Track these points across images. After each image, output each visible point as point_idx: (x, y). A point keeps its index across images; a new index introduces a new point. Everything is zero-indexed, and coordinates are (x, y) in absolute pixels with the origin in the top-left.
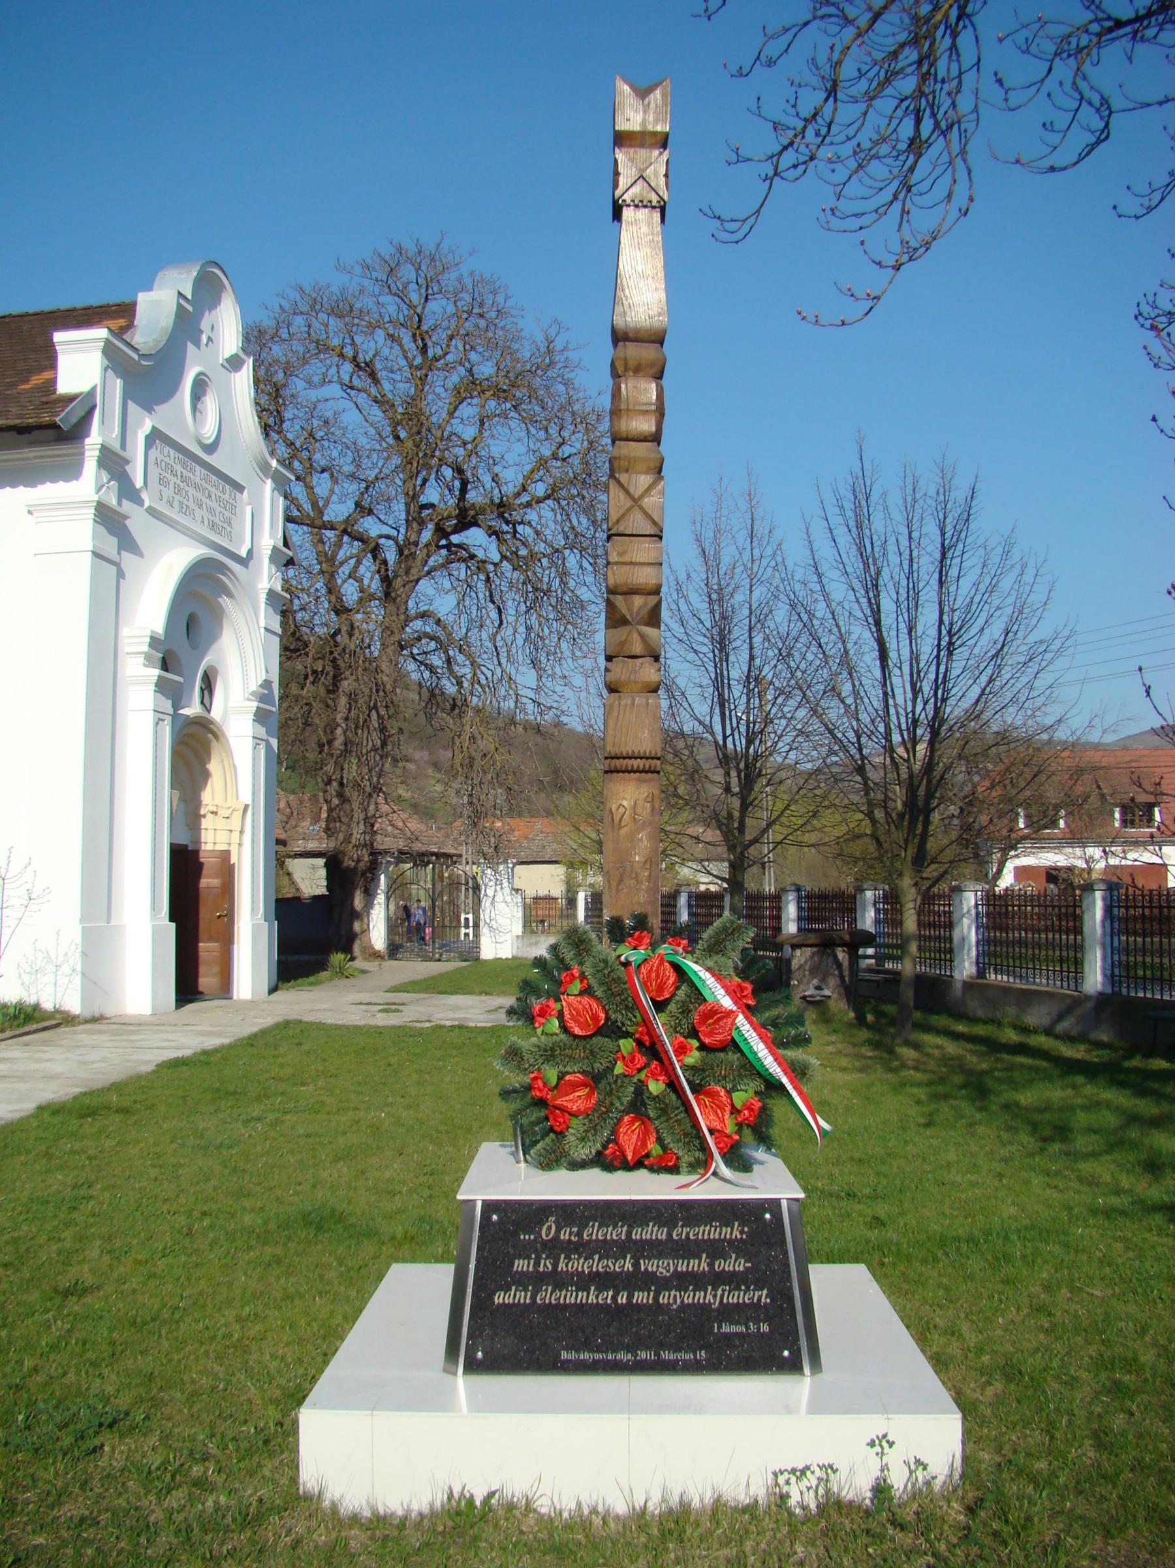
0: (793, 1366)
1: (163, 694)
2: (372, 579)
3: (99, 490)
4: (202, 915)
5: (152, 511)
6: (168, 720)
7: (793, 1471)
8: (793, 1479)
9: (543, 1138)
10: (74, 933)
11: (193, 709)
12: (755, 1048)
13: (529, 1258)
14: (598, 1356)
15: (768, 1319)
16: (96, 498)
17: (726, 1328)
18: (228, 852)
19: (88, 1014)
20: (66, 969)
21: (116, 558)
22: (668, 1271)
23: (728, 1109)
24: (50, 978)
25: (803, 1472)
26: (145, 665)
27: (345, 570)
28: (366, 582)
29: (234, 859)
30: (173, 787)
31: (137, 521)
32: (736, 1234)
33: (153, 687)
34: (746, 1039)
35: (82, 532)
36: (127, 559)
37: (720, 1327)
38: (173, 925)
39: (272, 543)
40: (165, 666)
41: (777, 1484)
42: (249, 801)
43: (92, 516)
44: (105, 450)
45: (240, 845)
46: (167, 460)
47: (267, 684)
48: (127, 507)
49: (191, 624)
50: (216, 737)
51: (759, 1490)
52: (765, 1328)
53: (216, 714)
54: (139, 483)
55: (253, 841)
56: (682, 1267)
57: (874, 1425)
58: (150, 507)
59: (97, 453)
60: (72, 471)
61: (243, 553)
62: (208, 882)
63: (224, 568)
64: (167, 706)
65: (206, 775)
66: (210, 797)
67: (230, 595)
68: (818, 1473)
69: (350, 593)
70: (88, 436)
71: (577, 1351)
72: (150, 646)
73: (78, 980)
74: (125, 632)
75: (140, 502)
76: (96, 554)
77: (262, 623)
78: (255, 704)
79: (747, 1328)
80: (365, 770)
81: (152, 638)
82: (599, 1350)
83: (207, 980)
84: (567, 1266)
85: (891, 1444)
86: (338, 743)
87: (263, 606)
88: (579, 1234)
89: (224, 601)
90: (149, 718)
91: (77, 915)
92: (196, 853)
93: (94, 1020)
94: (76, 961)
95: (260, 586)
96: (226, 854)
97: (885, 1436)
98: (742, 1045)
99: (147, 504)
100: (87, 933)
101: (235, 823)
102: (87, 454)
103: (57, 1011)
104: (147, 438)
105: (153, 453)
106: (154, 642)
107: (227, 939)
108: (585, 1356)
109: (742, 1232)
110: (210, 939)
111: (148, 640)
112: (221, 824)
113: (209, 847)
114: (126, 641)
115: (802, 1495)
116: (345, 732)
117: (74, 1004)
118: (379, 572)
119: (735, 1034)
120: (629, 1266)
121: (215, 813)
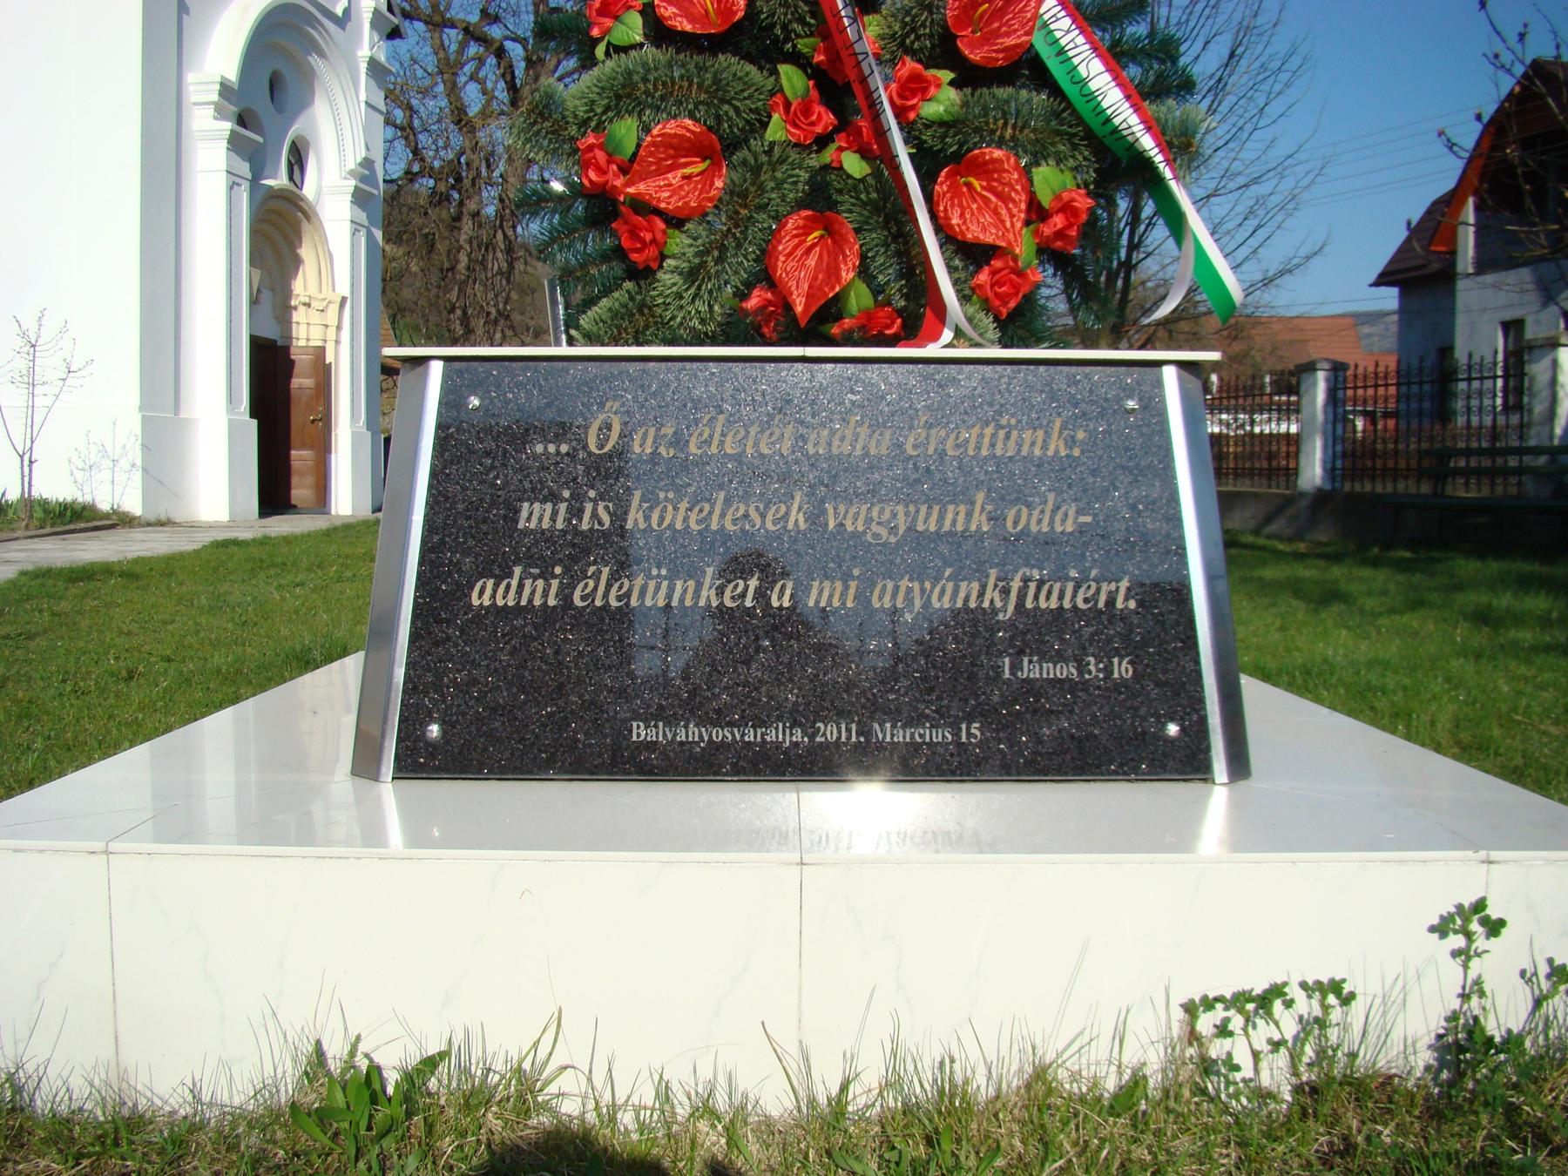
0: (1189, 763)
1: (238, 154)
2: (496, 82)
4: (293, 419)
6: (245, 186)
7: (1238, 1000)
8: (1237, 1022)
9: (606, 292)
10: (132, 423)
11: (278, 180)
12: (1082, 70)
13: (554, 497)
14: (720, 734)
15: (1135, 652)
17: (1032, 669)
18: (323, 349)
19: (152, 519)
20: (124, 464)
22: (893, 530)
23: (1021, 199)
24: (107, 475)
25: (1264, 1001)
27: (468, 69)
28: (489, 85)
29: (329, 358)
30: (253, 261)
32: (1057, 446)
33: (225, 144)
34: (1061, 52)
37: (1015, 667)
38: (255, 422)
39: (373, 4)
40: (241, 121)
41: (1193, 1036)
42: (348, 294)
45: (337, 342)
47: (367, 163)
49: (275, 85)
50: (308, 217)
51: (1148, 1050)
52: (1123, 669)
53: (309, 190)
55: (352, 339)
56: (928, 523)
57: (1453, 877)
61: (339, 11)
62: (301, 382)
63: (310, 19)
64: (244, 168)
65: (297, 262)
66: (303, 286)
67: (322, 54)
68: (1305, 1006)
69: (472, 96)
71: (671, 721)
72: (221, 94)
73: (138, 476)
74: (191, 78)
77: (363, 97)
78: (353, 183)
79: (1082, 667)
80: (491, 295)
81: (222, 84)
82: (718, 718)
83: (300, 492)
84: (647, 518)
85: (1494, 927)
86: (462, 266)
87: (363, 77)
88: (679, 441)
89: (314, 60)
90: (221, 181)
91: (135, 399)
92: (286, 349)
93: (161, 524)
94: (136, 454)
95: (360, 53)
96: (321, 351)
97: (1479, 906)
98: (1053, 65)
100: (146, 421)
101: (332, 316)
103: (115, 512)
106: (225, 89)
107: (323, 447)
108: (690, 733)
109: (1071, 442)
110: (303, 446)
112: (315, 317)
113: (302, 343)
114: (191, 88)
115: (1260, 1061)
116: (469, 255)
117: (133, 505)
118: (503, 75)
119: (1038, 42)
120: (797, 519)
121: (308, 305)
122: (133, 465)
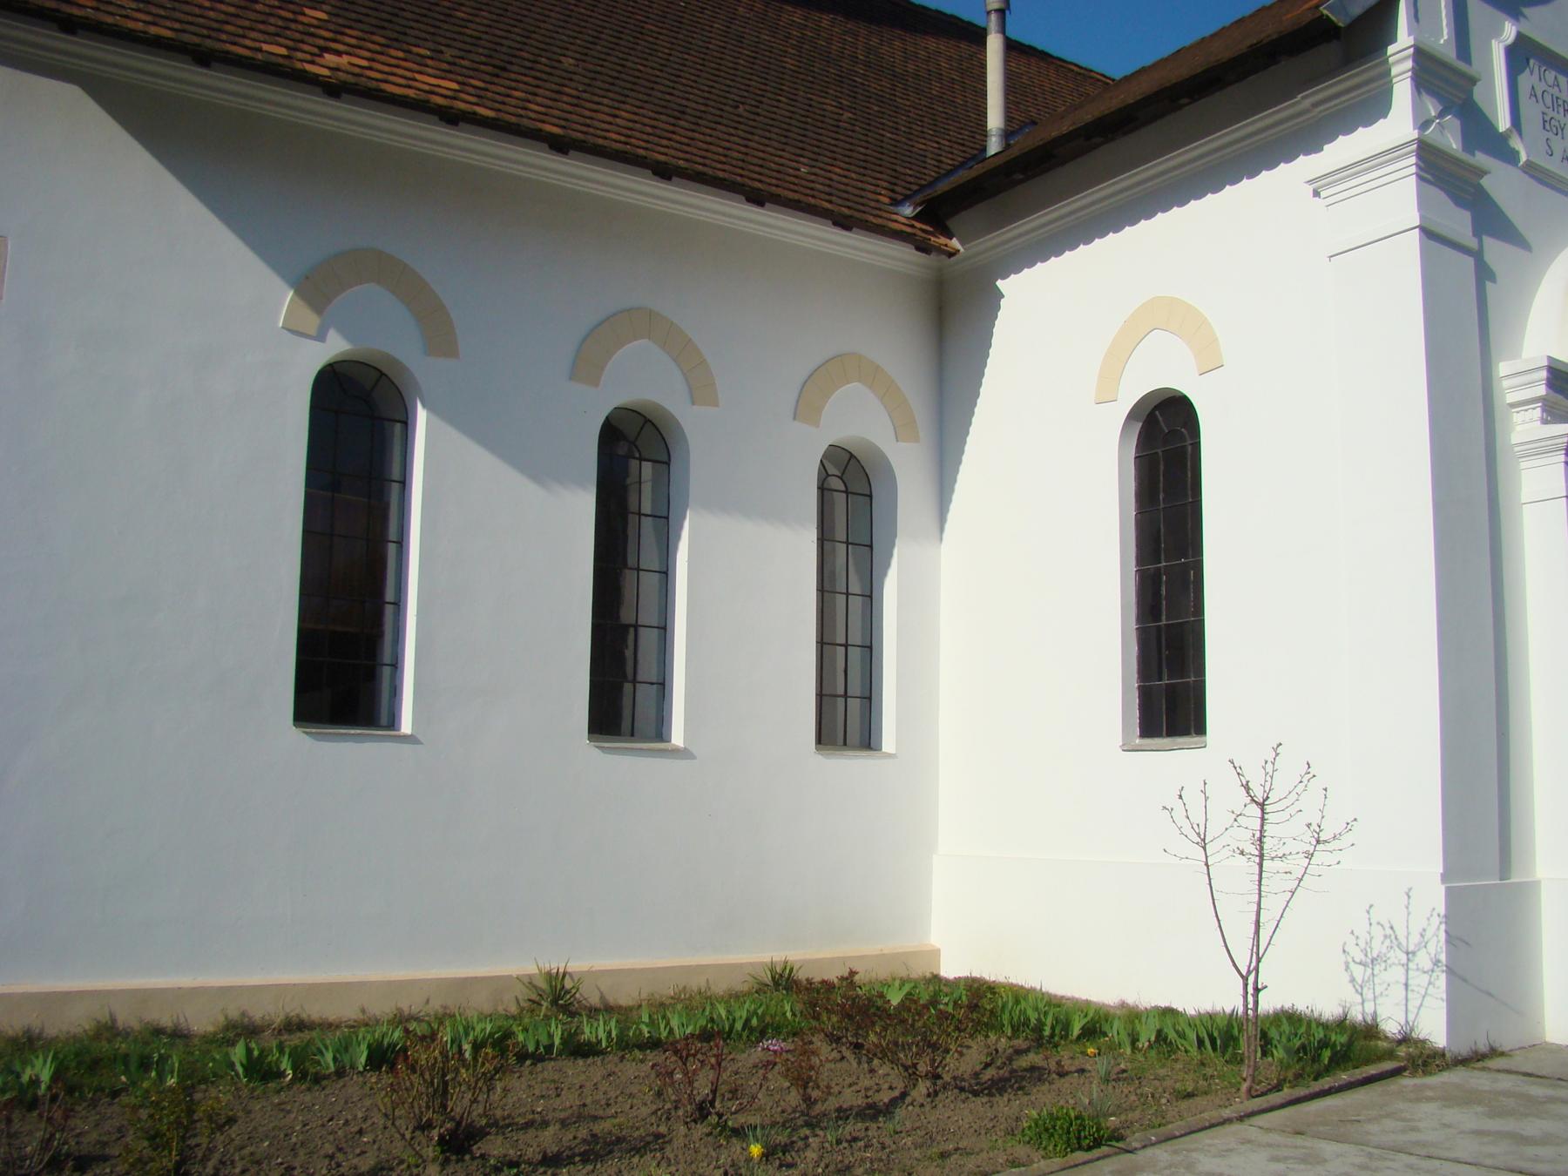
3: (1423, 125)
5: (1531, 169)
16: (1415, 134)
19: (1463, 1050)
20: (1422, 959)
21: (1472, 243)
24: (1397, 973)
26: (1544, 422)
31: (1501, 183)
35: (1399, 199)
36: (1494, 250)
43: (1413, 169)
44: (1423, 57)
46: (1555, 91)
48: (1481, 159)
54: (1503, 123)
58: (1529, 164)
59: (1409, 64)
60: (1375, 107)
70: (1393, 40)
73: (1441, 980)
74: (1503, 368)
75: (1511, 157)
76: (1427, 233)
91: (1438, 868)
93: (1473, 1059)
99: (1523, 158)
100: (1453, 897)
102: (1394, 71)
104: (1511, 52)
105: (1526, 80)
111: (1544, 374)
114: (1506, 383)
117: (1434, 1029)
122: (1437, 962)
